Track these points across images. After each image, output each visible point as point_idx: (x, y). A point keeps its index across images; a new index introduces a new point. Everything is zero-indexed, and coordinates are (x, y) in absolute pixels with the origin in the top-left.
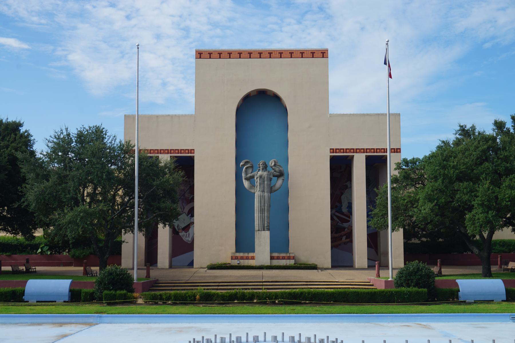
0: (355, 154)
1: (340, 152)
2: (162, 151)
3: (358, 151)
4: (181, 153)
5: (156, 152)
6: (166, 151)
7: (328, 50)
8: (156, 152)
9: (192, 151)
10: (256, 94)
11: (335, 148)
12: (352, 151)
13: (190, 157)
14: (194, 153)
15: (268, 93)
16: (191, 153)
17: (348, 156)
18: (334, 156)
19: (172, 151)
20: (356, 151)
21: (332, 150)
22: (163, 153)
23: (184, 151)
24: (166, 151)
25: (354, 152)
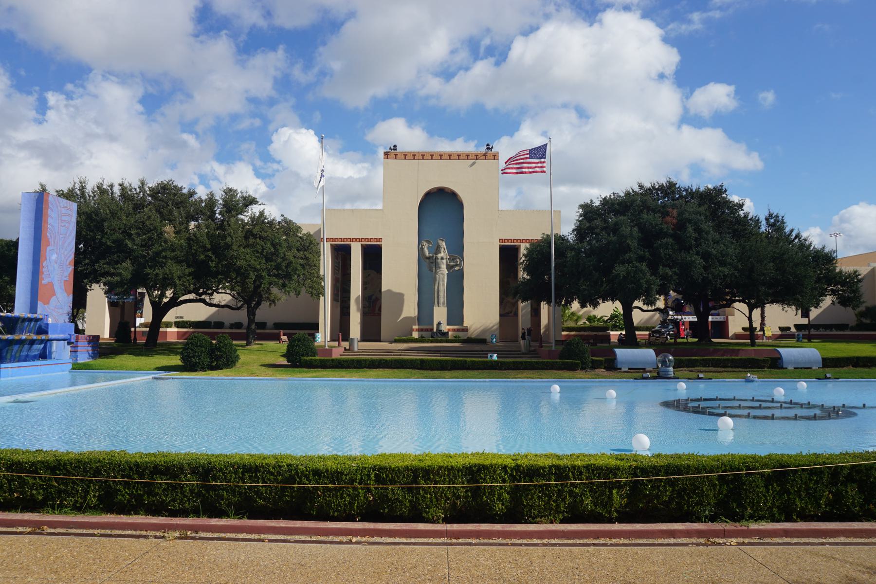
0: (521, 244)
1: (374, 241)
2: (354, 240)
3: (524, 241)
4: (370, 241)
5: (349, 240)
6: (358, 240)
7: (498, 153)
8: (349, 240)
9: (380, 240)
10: (435, 190)
11: (504, 238)
12: (519, 241)
13: (378, 245)
14: (381, 241)
15: (446, 190)
16: (379, 242)
17: (516, 245)
18: (503, 245)
19: (363, 240)
20: (352, 240)
21: (501, 240)
22: (355, 242)
23: (374, 239)
24: (358, 240)
25: (520, 242)
